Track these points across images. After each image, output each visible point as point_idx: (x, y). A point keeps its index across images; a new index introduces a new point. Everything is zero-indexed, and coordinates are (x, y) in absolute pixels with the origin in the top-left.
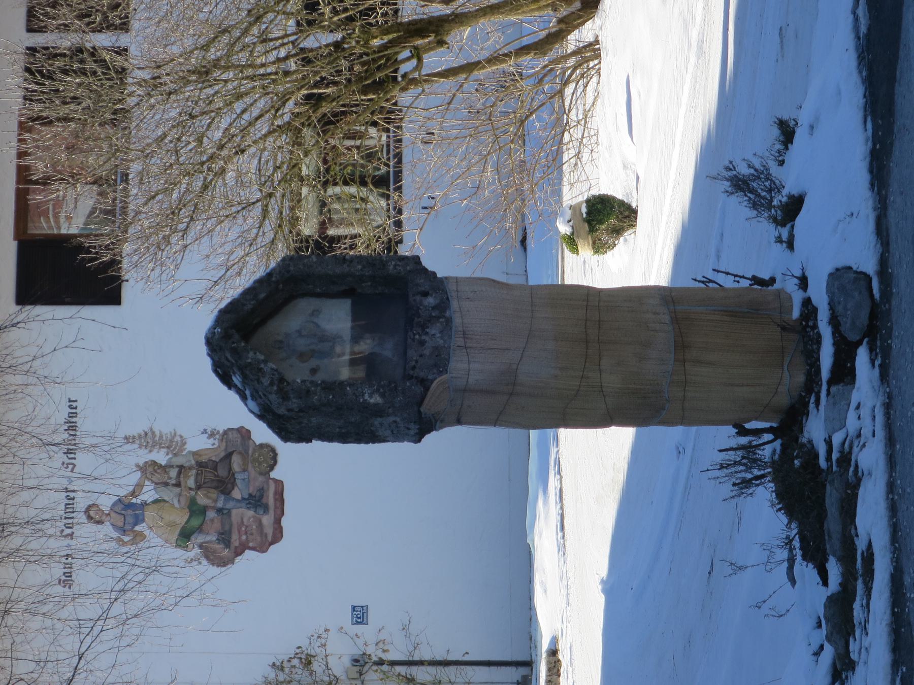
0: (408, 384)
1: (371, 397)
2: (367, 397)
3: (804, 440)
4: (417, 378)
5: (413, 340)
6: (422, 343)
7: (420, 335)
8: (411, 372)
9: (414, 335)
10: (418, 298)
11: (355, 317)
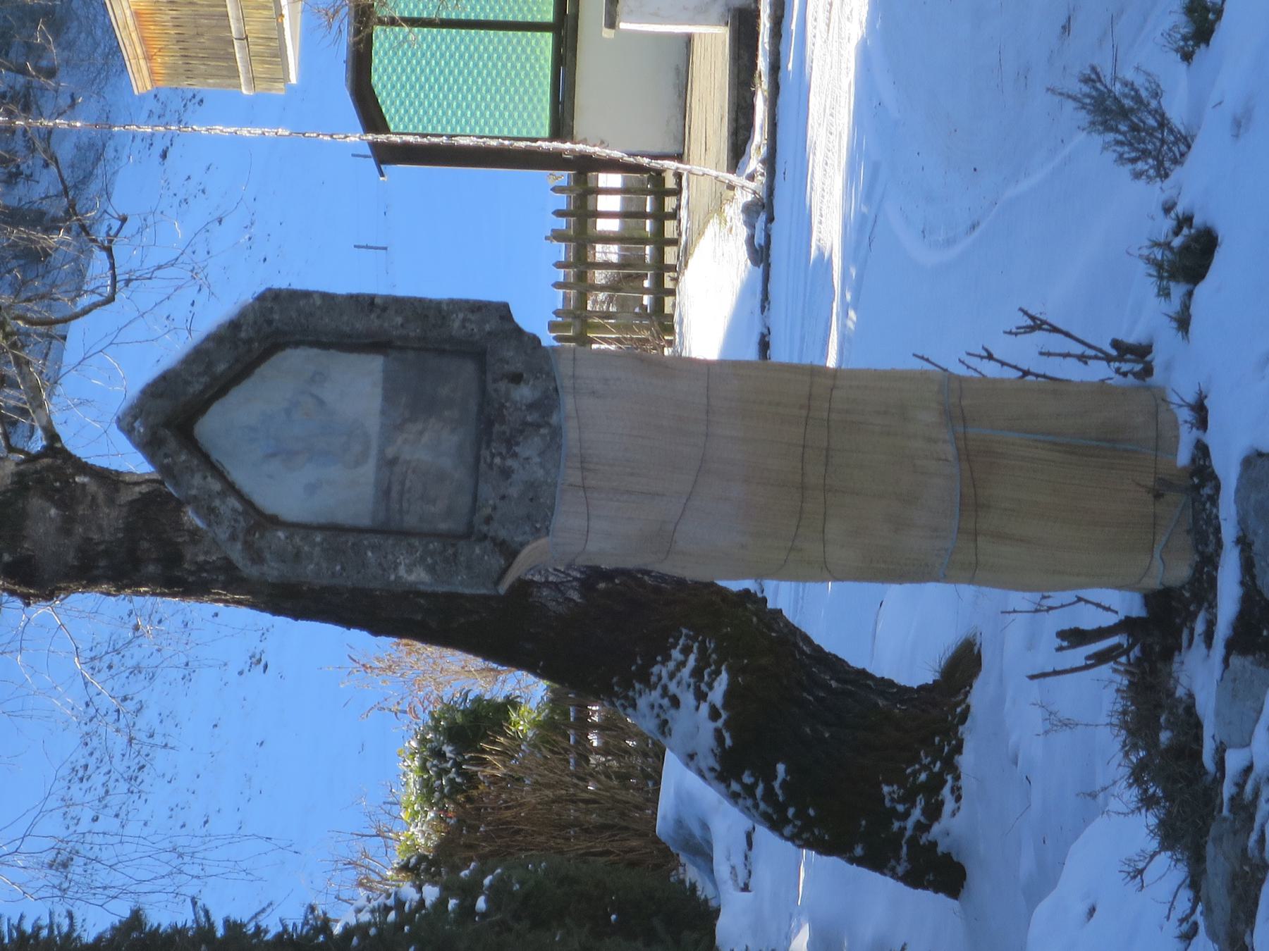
0: (478, 551)
1: (409, 571)
2: (402, 571)
3: (1180, 692)
4: (494, 540)
5: (491, 466)
6: (506, 473)
7: (503, 458)
8: (485, 528)
9: (493, 456)
10: (502, 386)
11: (389, 396)
